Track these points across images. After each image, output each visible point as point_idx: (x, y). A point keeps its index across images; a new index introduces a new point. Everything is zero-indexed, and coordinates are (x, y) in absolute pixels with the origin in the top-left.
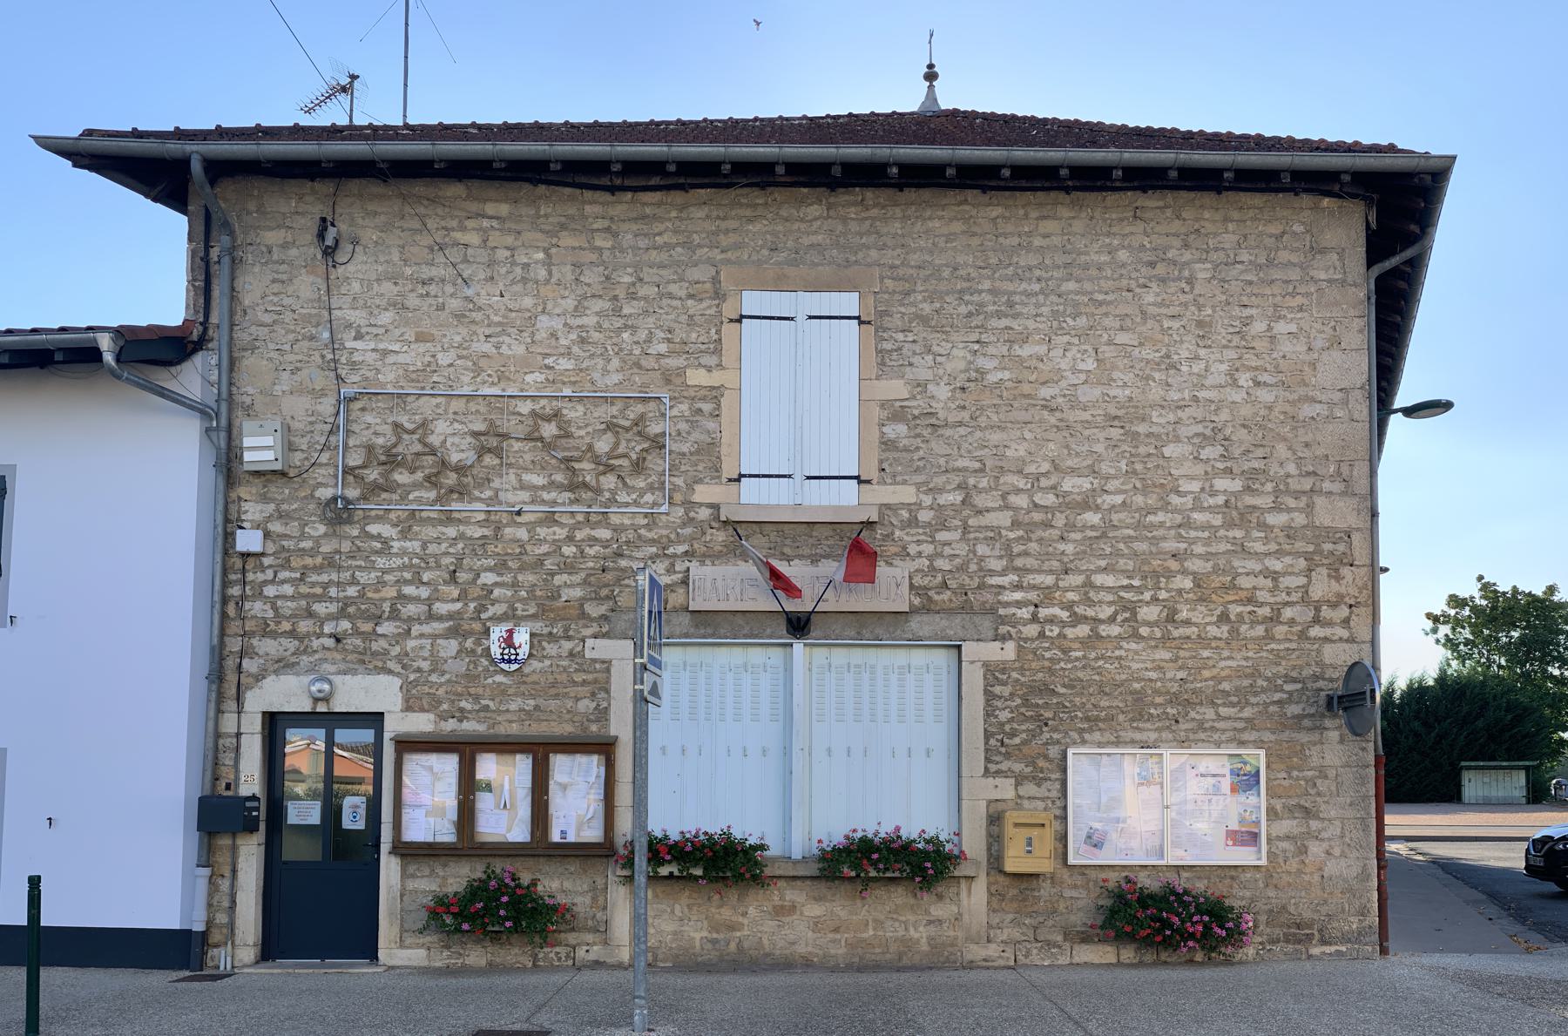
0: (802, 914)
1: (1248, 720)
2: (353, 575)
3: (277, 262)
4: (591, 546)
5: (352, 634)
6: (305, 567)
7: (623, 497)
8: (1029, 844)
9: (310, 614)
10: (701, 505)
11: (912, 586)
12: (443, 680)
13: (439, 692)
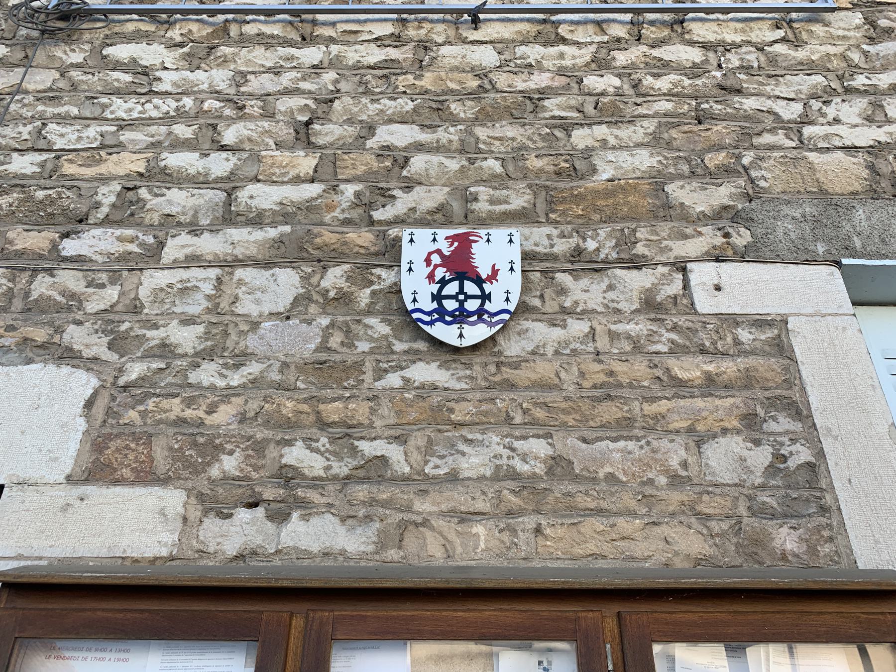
2: (39, 133)
12: (236, 379)
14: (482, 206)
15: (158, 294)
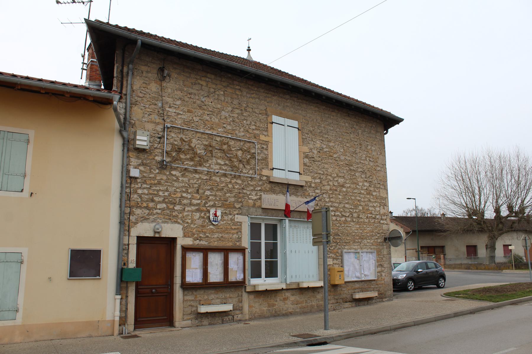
0: (289, 300)
1: (372, 243)
2: (167, 188)
3: (145, 77)
4: (236, 185)
5: (166, 209)
6: (151, 184)
7: (244, 171)
8: (340, 276)
9: (153, 201)
10: (264, 176)
12: (195, 226)
13: (194, 231)
14: (217, 205)
15: (186, 215)
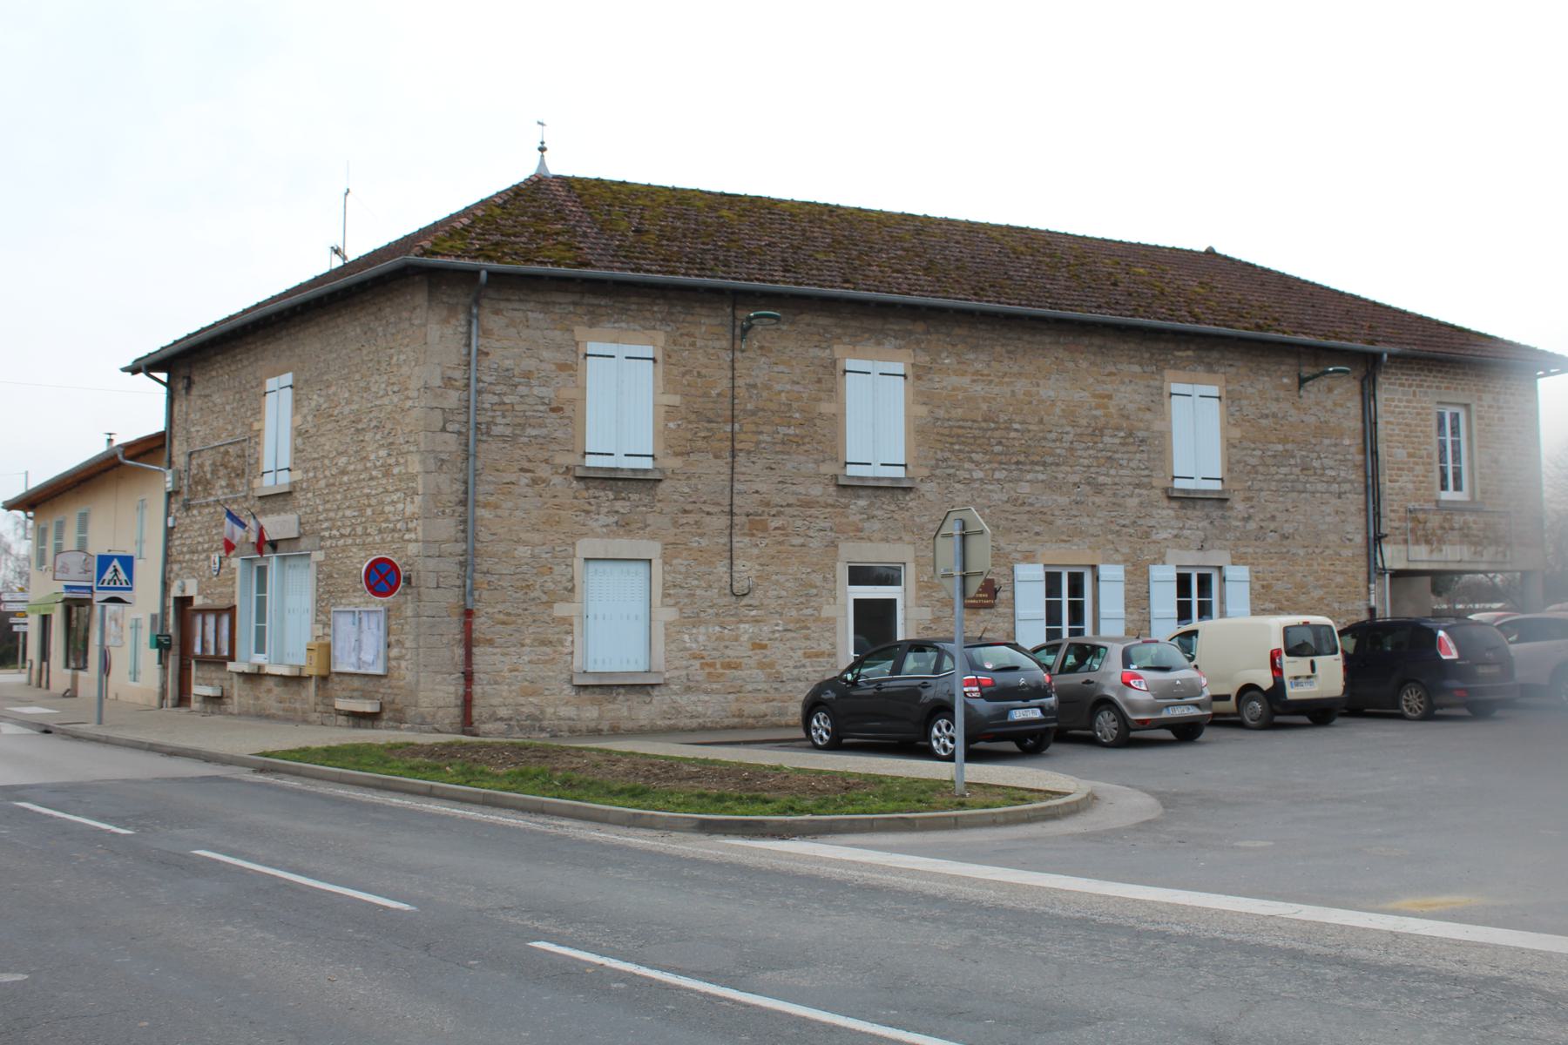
11: (301, 524)
